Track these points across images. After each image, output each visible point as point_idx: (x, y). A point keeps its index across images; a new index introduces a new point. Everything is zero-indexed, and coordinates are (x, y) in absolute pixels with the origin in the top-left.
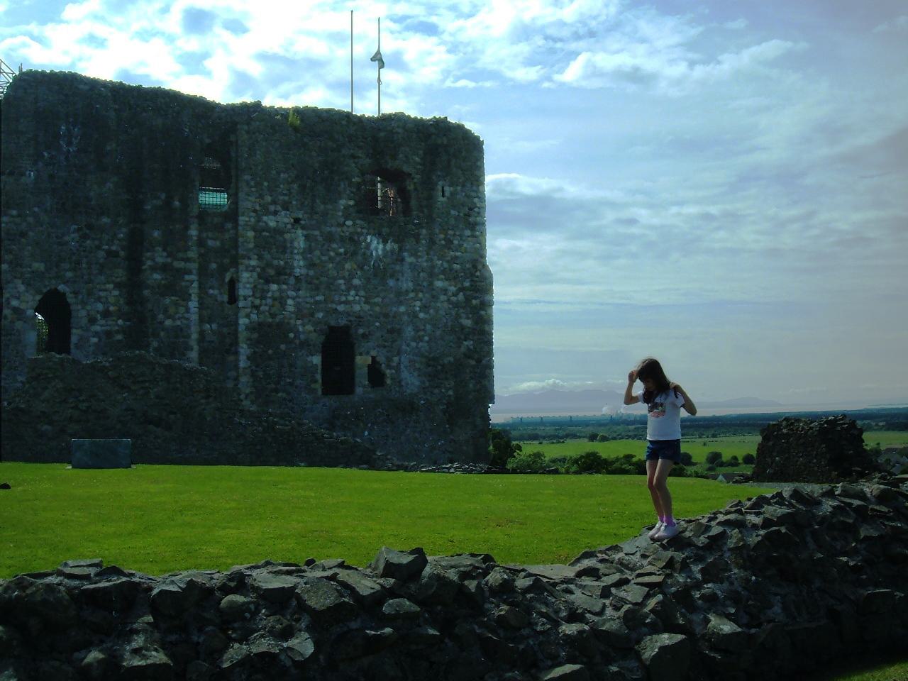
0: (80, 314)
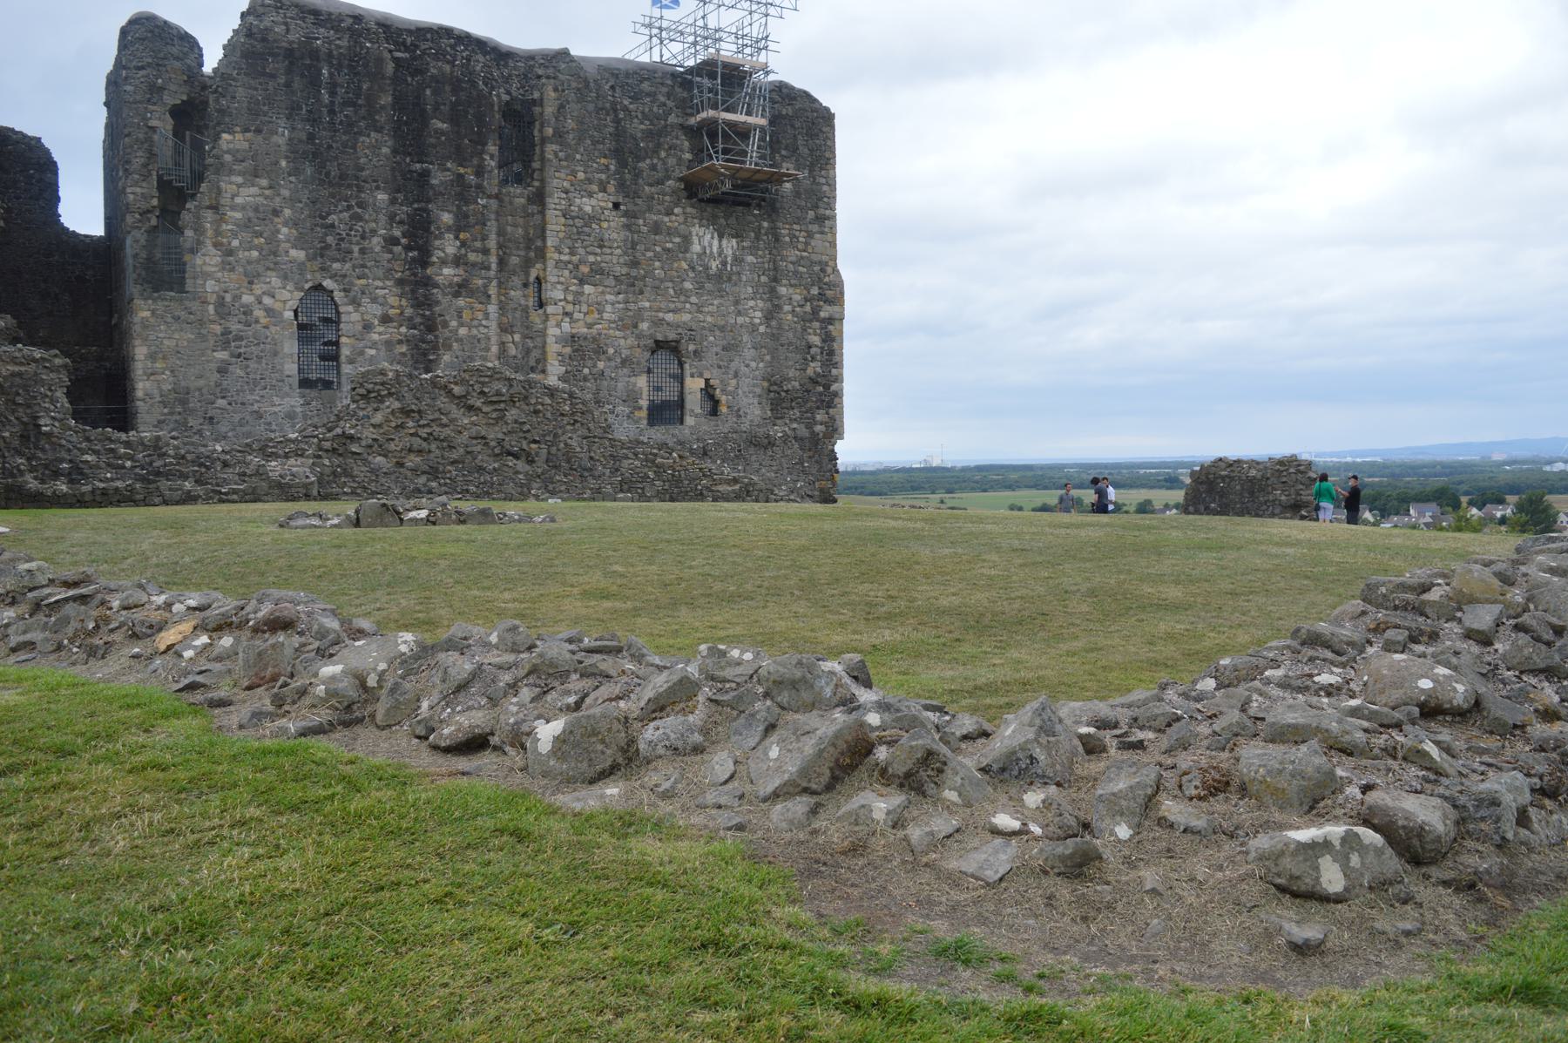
0: (351, 318)
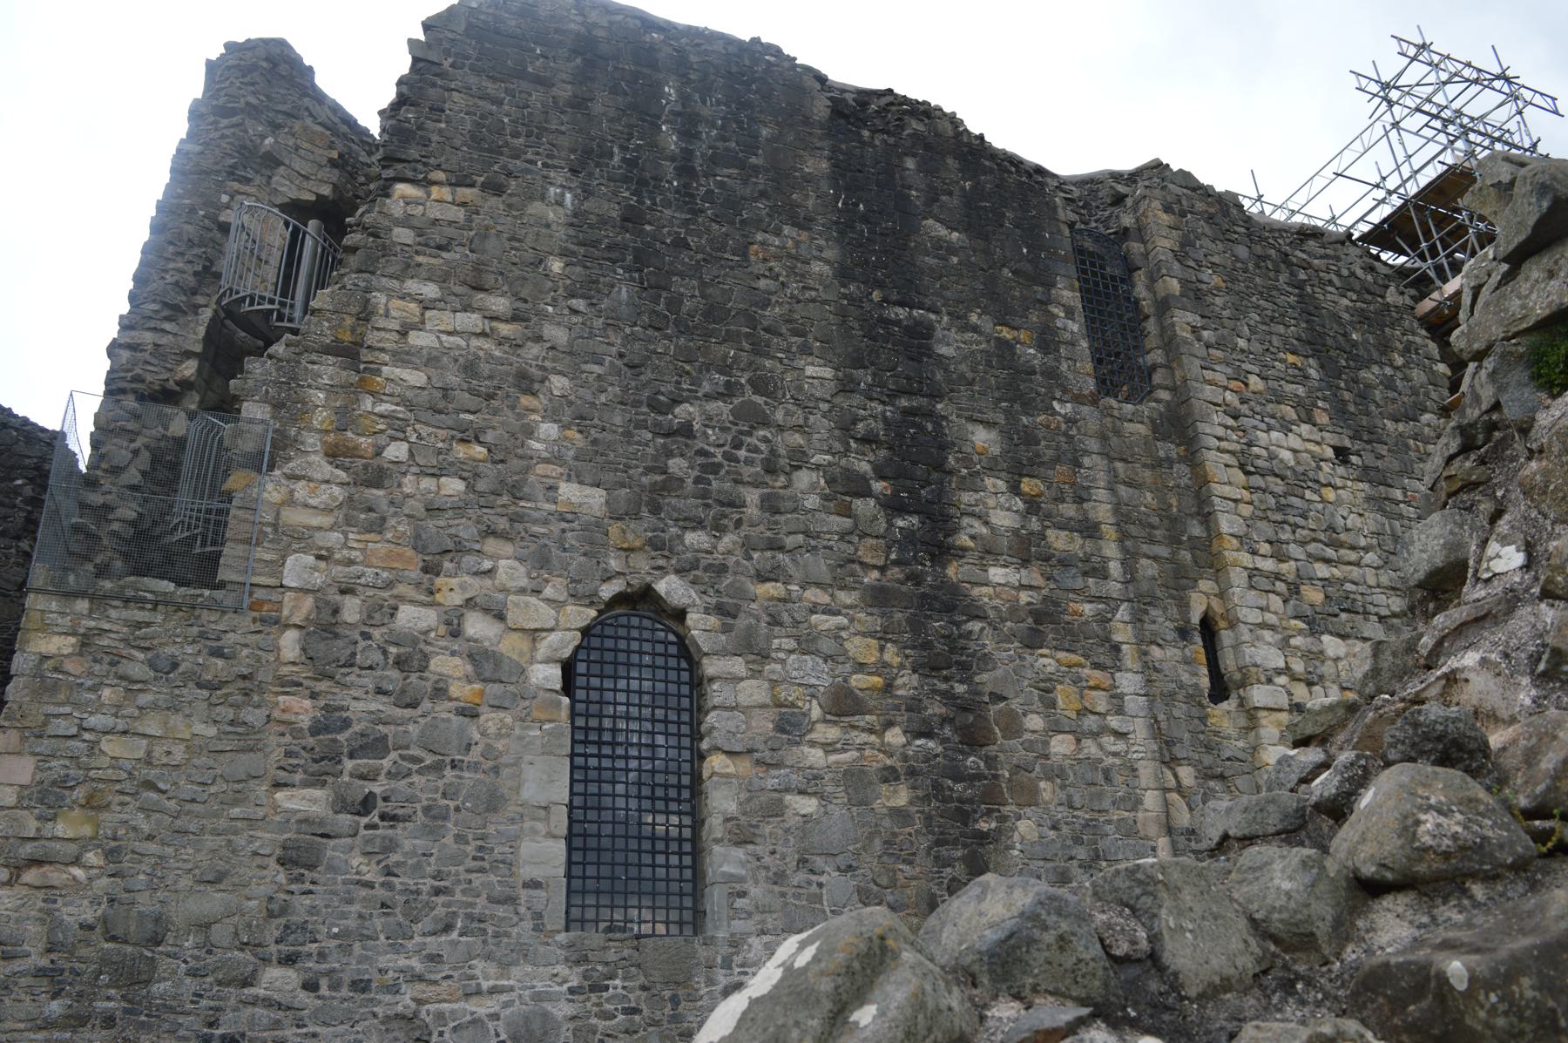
0: (738, 695)
